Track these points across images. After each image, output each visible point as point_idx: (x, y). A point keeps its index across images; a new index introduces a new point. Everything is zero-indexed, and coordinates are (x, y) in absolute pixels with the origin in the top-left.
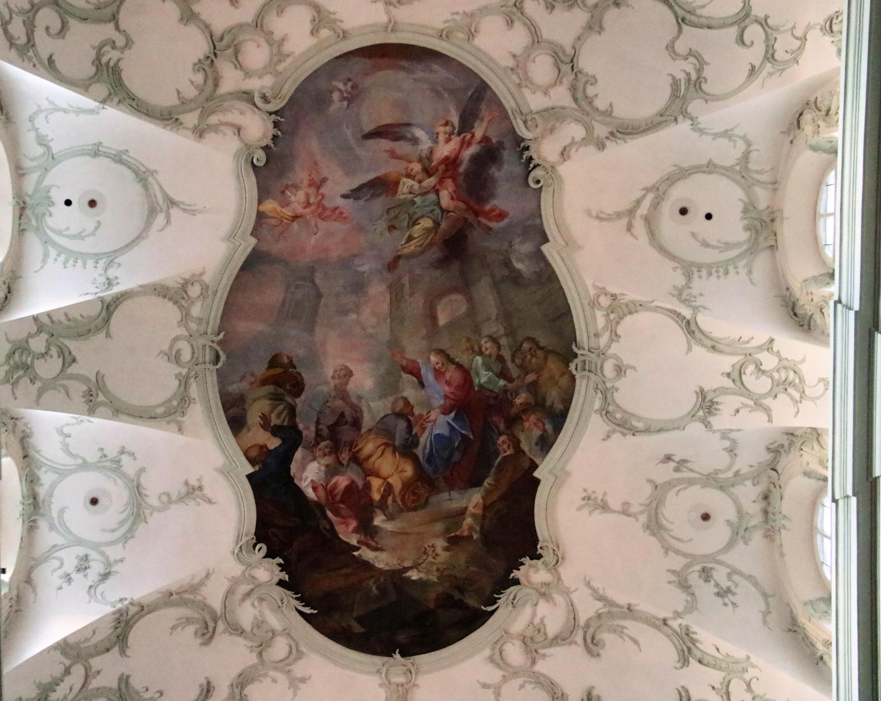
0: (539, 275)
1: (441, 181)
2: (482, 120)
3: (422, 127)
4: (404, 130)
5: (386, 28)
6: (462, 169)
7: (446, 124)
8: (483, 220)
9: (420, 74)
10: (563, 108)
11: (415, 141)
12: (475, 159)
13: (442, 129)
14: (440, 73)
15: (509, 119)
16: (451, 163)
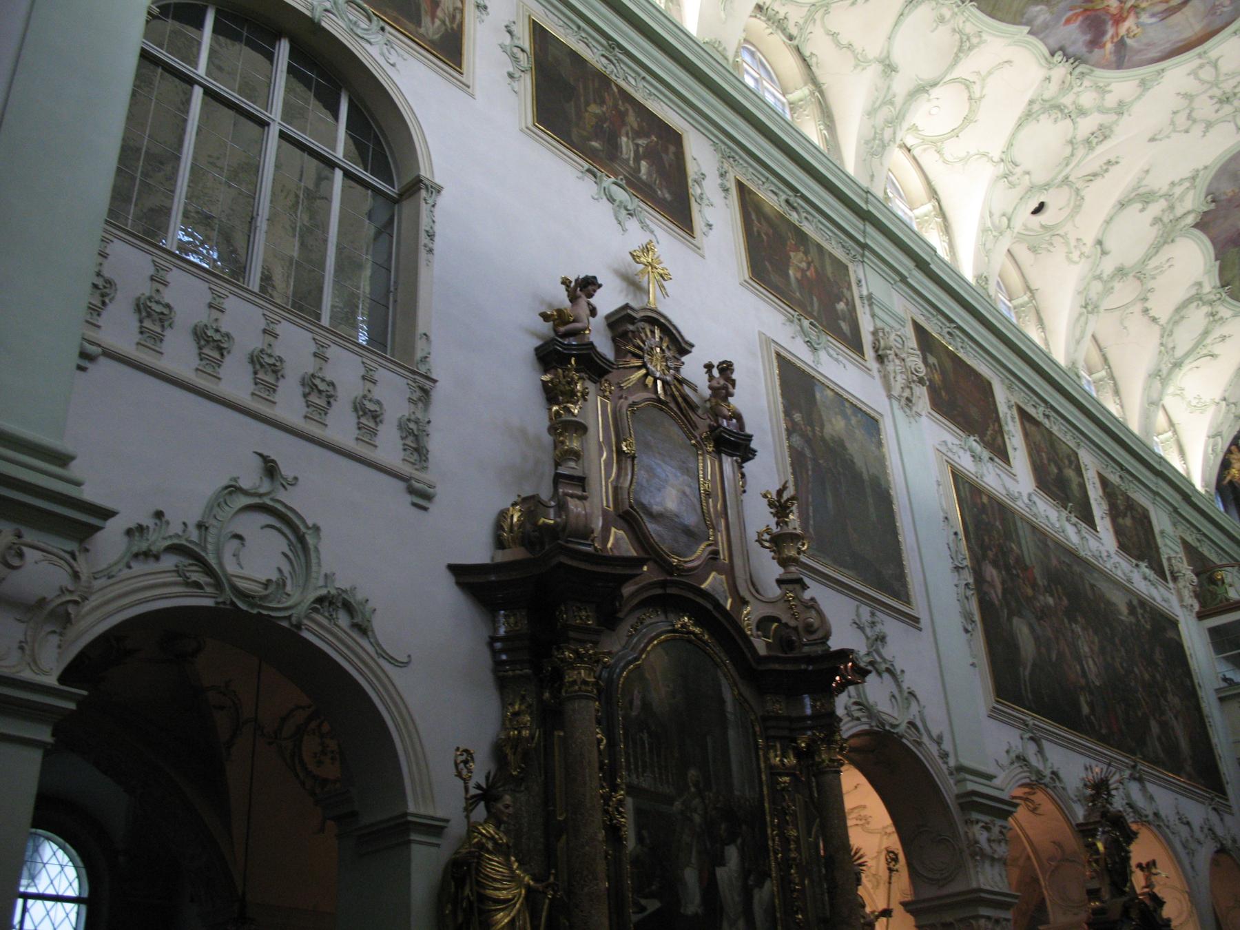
0: (1022, 15)
1: (1122, 8)
2: (1111, 53)
3: (1151, 24)
4: (1164, 15)
5: (1205, 52)
6: (1110, 23)
7: (1134, 36)
8: (1078, 11)
9: (1168, 45)
10: (1064, 96)
11: (1153, 15)
12: (1104, 33)
13: (1136, 32)
14: (1154, 54)
15: (1093, 66)
16: (1118, 20)
